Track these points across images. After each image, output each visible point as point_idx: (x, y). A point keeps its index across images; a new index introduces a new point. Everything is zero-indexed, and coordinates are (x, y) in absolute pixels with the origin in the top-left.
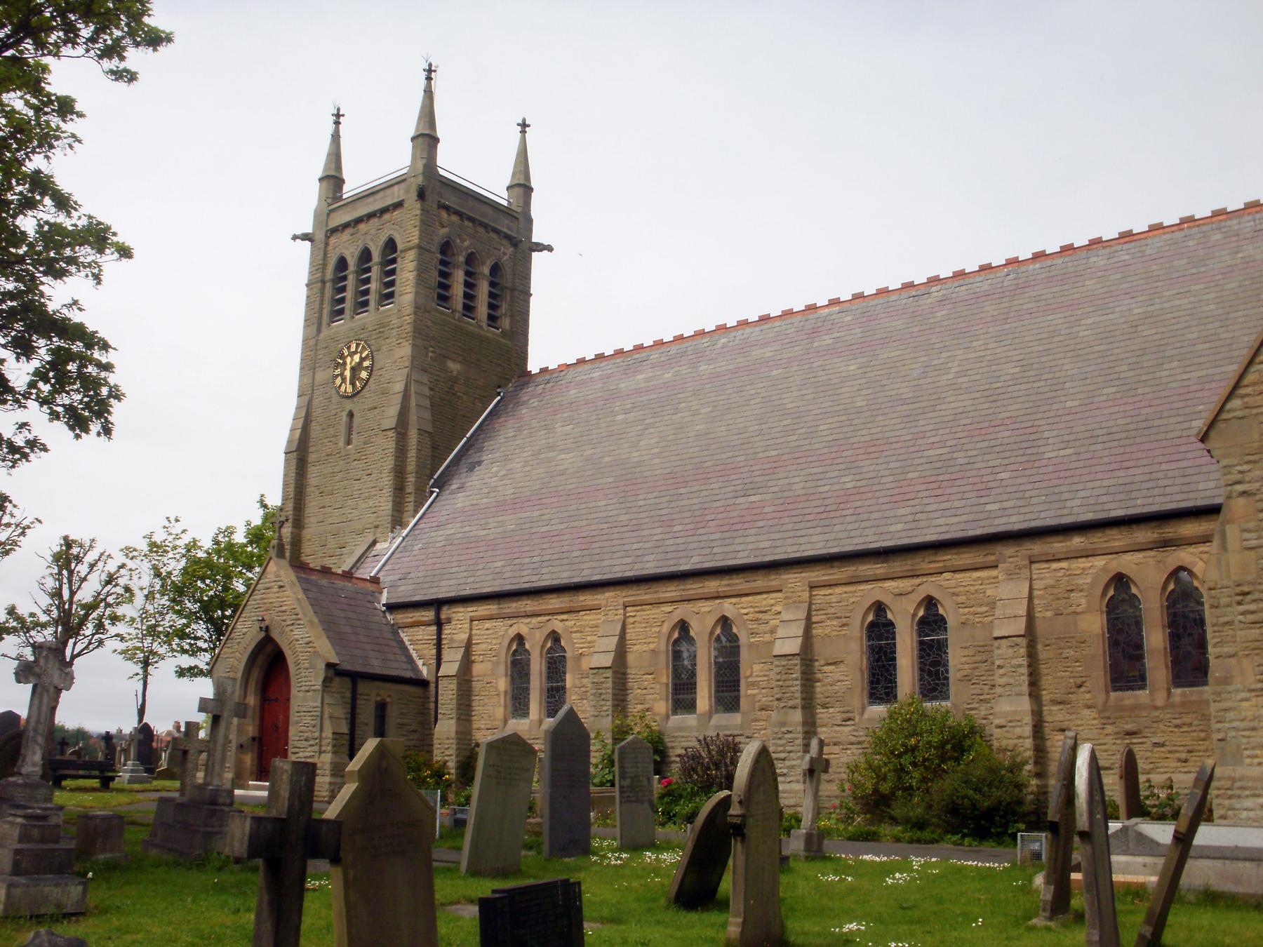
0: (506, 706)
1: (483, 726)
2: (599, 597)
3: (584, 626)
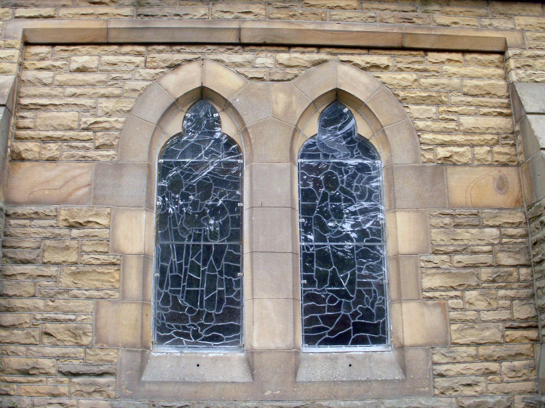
0: (144, 302)
1: (47, 364)
2: (495, 23)
3: (451, 91)
